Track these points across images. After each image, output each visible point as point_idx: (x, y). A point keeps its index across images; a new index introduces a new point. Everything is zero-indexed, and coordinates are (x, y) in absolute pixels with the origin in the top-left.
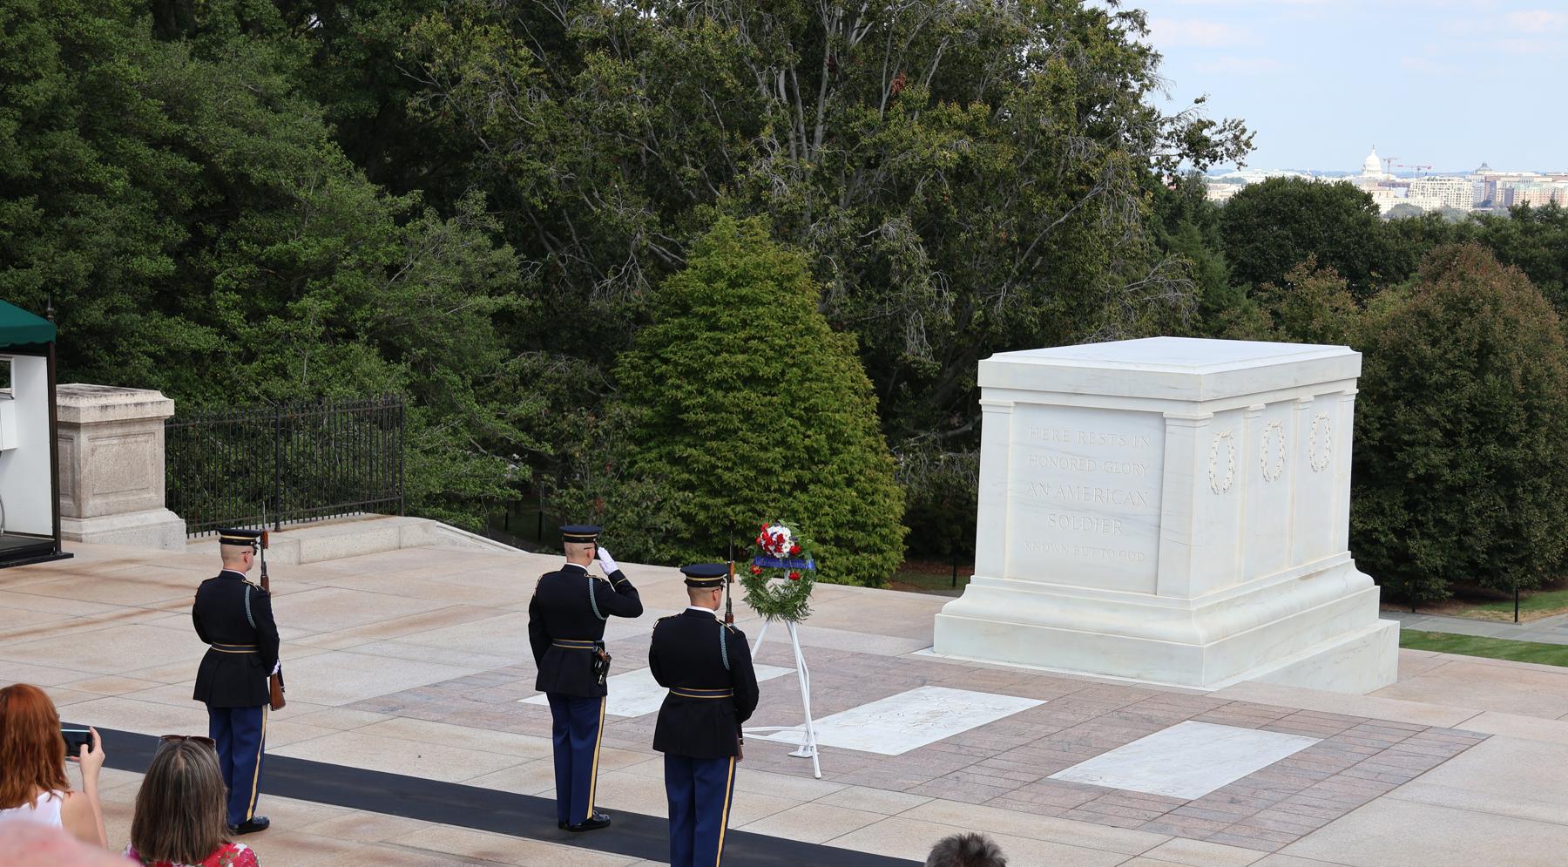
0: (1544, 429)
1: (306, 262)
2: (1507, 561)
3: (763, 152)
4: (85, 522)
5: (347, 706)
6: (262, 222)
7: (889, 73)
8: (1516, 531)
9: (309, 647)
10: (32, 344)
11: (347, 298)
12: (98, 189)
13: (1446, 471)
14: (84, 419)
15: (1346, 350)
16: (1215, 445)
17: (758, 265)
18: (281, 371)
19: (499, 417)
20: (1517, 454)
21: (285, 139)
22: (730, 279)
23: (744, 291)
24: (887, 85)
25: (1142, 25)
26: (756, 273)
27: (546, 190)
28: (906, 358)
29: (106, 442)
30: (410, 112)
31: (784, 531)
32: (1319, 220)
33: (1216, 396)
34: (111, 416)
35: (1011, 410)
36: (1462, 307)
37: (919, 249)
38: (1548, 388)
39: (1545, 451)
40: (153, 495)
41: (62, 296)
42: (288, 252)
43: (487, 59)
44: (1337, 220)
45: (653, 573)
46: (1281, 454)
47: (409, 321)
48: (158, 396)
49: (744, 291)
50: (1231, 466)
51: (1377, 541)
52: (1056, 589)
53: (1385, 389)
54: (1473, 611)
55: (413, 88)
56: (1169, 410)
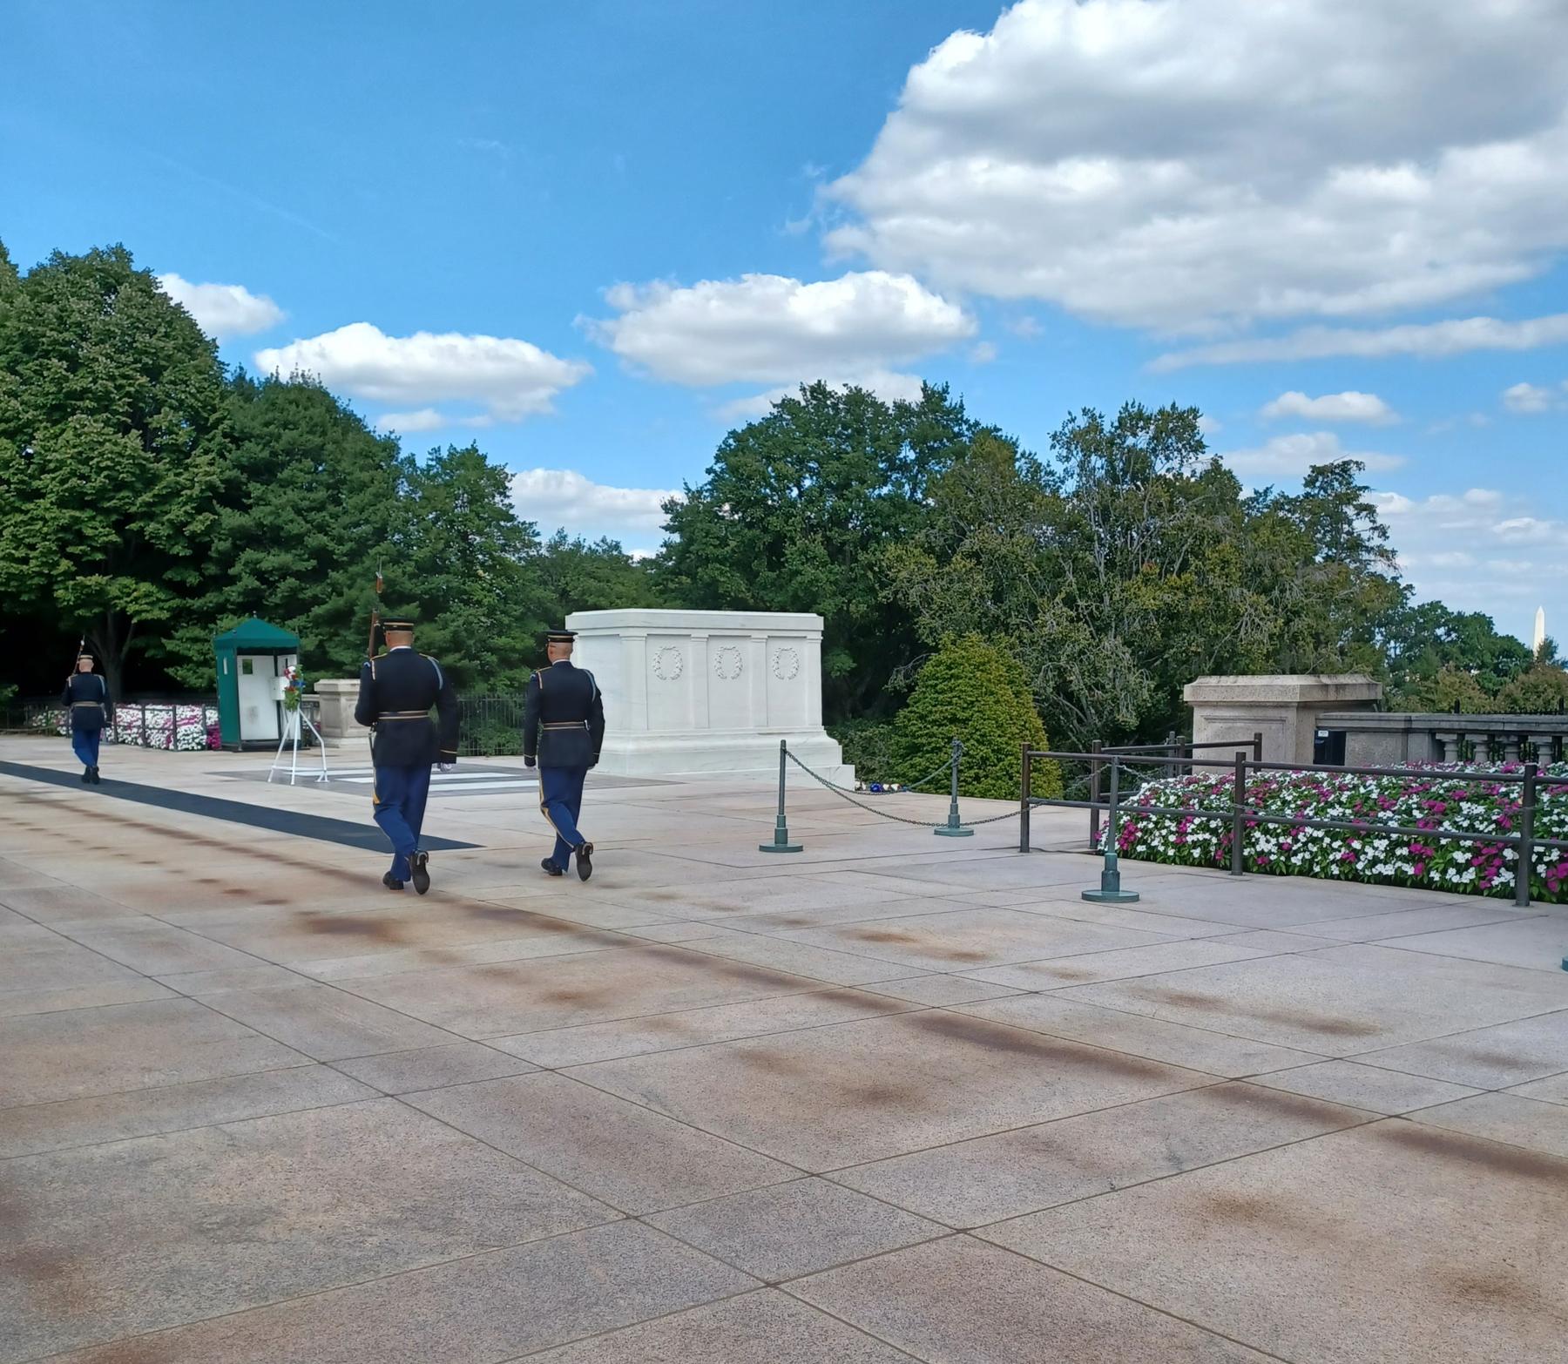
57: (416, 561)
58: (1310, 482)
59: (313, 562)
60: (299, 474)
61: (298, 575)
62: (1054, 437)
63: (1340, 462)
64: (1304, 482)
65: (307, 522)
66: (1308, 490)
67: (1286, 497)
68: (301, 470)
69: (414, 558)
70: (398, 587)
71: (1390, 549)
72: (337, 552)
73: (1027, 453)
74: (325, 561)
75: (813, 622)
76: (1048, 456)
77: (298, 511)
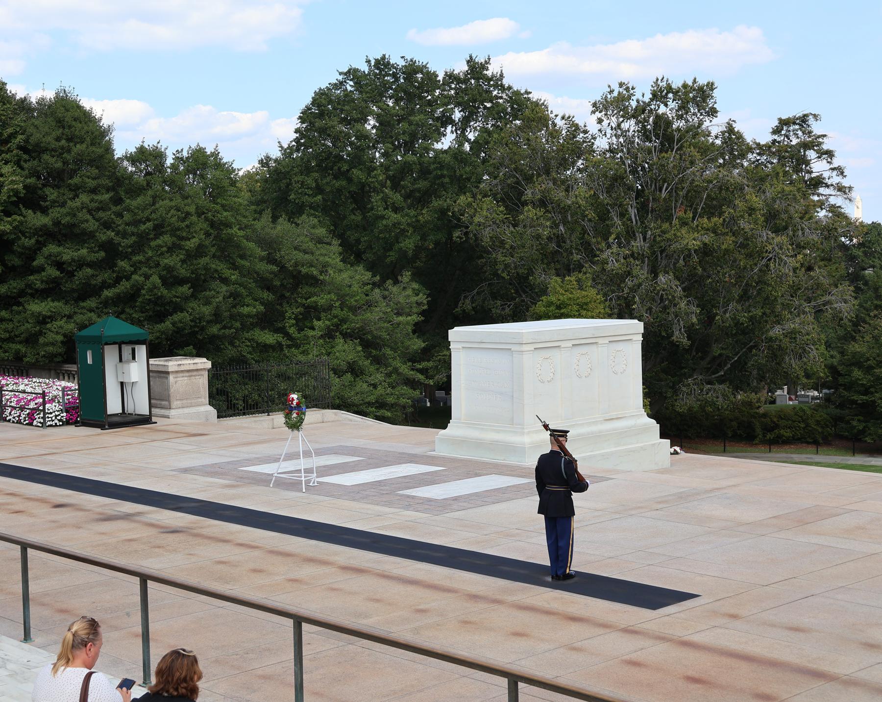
1: (321, 305)
3: (609, 246)
4: (172, 411)
6: (306, 289)
9: (194, 452)
10: (138, 340)
12: (225, 281)
14: (170, 370)
16: (539, 362)
17: (570, 298)
18: (305, 353)
19: (413, 370)
21: (321, 255)
22: (557, 305)
23: (562, 311)
24: (675, 211)
28: (673, 340)
29: (182, 379)
31: (294, 396)
33: (534, 341)
34: (182, 368)
35: (461, 350)
37: (678, 288)
40: (203, 400)
41: (200, 323)
42: (315, 302)
45: (416, 430)
46: (590, 365)
47: (370, 329)
48: (204, 360)
49: (562, 311)
50: (553, 370)
52: (479, 424)
55: (457, 226)
56: (514, 348)
57: (187, 251)
59: (102, 254)
60: (87, 180)
61: (91, 265)
62: (594, 105)
65: (97, 220)
69: (187, 248)
70: (175, 273)
72: (123, 244)
74: (112, 251)
75: (634, 328)
77: (90, 212)
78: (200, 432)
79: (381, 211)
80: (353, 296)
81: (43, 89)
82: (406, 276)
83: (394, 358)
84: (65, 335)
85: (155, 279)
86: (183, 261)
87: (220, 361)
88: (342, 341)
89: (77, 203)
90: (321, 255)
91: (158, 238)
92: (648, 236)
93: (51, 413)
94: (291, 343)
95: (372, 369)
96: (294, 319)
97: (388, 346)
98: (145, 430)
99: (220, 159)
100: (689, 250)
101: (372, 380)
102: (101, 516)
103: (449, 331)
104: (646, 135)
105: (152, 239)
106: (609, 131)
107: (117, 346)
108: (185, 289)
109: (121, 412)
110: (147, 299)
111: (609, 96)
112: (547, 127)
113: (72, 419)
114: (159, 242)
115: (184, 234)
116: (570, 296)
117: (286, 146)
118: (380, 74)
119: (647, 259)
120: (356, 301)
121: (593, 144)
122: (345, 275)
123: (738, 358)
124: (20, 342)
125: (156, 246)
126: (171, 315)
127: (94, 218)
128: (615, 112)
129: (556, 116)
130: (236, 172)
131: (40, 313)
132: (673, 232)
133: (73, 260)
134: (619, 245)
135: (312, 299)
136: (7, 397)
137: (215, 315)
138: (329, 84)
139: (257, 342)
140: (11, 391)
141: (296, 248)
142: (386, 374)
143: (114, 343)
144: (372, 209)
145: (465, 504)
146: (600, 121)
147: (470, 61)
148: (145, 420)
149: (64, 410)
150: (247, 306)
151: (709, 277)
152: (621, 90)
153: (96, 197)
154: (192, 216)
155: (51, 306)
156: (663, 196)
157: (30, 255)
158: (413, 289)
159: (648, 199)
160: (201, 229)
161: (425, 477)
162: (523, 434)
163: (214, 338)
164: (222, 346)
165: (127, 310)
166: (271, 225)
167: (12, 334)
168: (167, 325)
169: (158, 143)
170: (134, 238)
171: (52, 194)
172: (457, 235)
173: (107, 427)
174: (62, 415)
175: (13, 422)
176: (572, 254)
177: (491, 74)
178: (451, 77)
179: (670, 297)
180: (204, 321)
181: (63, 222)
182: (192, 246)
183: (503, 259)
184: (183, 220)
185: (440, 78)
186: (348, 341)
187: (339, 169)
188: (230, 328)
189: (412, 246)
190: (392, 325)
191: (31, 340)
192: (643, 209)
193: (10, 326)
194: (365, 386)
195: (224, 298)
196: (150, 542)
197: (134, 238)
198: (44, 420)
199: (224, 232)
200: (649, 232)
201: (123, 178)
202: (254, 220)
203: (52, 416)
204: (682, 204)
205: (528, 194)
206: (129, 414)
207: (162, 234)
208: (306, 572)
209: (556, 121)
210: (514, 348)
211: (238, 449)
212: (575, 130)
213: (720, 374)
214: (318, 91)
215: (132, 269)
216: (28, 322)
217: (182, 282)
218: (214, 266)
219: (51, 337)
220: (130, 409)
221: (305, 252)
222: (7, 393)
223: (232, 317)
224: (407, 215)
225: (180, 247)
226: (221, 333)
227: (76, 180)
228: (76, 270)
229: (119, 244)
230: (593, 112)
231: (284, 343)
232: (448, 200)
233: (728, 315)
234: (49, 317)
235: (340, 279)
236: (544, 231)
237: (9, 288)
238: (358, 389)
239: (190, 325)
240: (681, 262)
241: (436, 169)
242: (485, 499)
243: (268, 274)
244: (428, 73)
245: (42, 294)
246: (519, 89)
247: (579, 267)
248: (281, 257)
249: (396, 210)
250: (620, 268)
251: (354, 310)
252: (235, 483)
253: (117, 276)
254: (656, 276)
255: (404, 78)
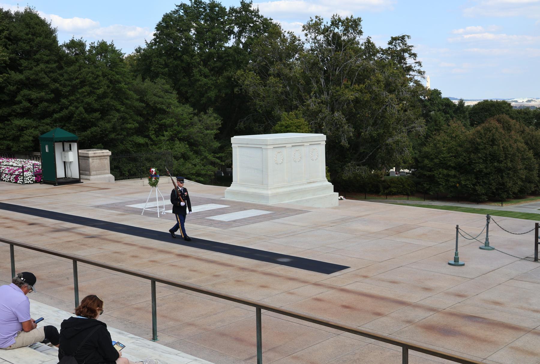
0: (509, 159)
2: (502, 191)
3: (311, 98)
4: (91, 176)
5: (91, 206)
6: (160, 116)
7: (343, 79)
8: (503, 184)
11: (177, 132)
12: (118, 111)
13: (485, 170)
15: (322, 135)
17: (292, 123)
18: (160, 148)
19: (214, 157)
20: (502, 165)
21: (168, 98)
23: (288, 129)
25: (420, 65)
26: (291, 125)
27: (262, 108)
29: (95, 160)
30: (235, 92)
31: (153, 170)
32: (496, 110)
33: (273, 144)
34: (96, 155)
36: (488, 130)
38: (510, 149)
39: (509, 164)
40: (107, 171)
41: (105, 132)
42: (164, 122)
43: (250, 79)
44: (501, 110)
46: (300, 156)
48: (108, 151)
49: (288, 129)
50: (282, 158)
51: (468, 187)
53: (469, 150)
54: (493, 204)
55: (236, 86)
56: (263, 147)
57: (98, 95)
58: (390, 43)
59: (53, 95)
60: (44, 56)
61: (47, 101)
62: (304, 27)
63: (401, 35)
64: (388, 43)
65: (50, 78)
66: (390, 46)
67: (382, 49)
68: (44, 55)
69: (98, 93)
70: (92, 106)
71: (422, 71)
72: (64, 91)
73: (290, 32)
74: (58, 95)
76: (300, 33)
77: (45, 73)
78: (106, 187)
79: (198, 77)
80: (184, 120)
81: (18, 7)
82: (210, 110)
83: (205, 152)
84: (34, 137)
85: (81, 109)
86: (96, 100)
87: (116, 152)
88: (178, 142)
89: (39, 68)
90: (168, 98)
91: (82, 88)
92: (330, 93)
93: (27, 177)
94: (152, 143)
95: (194, 156)
96: (154, 131)
97: (202, 145)
98: (77, 186)
99: (115, 48)
100: (349, 100)
101: (193, 162)
102: (53, 230)
103: (231, 138)
104: (328, 43)
105: (79, 88)
106: (311, 40)
107: (62, 143)
108: (97, 115)
109: (64, 176)
110: (77, 119)
111: (311, 23)
112: (281, 37)
113: (38, 180)
114: (83, 90)
115: (96, 86)
116: (292, 122)
117: (149, 42)
118: (197, 7)
119: (329, 104)
120: (185, 122)
121: (303, 46)
122: (179, 109)
123: (372, 153)
124: (10, 140)
125: (82, 92)
126: (90, 128)
127: (48, 76)
128: (314, 31)
129: (285, 32)
130: (123, 55)
131: (20, 126)
132: (341, 91)
133: (37, 98)
134: (316, 97)
135: (163, 121)
136: (3, 168)
137: (113, 128)
138: (171, 11)
139: (135, 142)
140: (5, 165)
141: (154, 95)
142: (201, 159)
143: (60, 141)
144: (193, 76)
145: (239, 224)
146: (306, 35)
147: (242, 3)
148: (77, 181)
149: (34, 176)
150: (130, 124)
151: (358, 114)
152: (317, 20)
153: (48, 66)
154: (100, 77)
155: (26, 122)
156: (337, 73)
157: (14, 94)
158: (214, 117)
159: (330, 75)
160: (105, 84)
161: (220, 210)
162: (268, 189)
163: (113, 139)
164: (117, 144)
165: (67, 125)
166: (142, 83)
167: (5, 136)
168: (88, 132)
169: (82, 38)
170: (69, 88)
171: (25, 63)
172: (236, 90)
173: (57, 184)
174: (33, 178)
175: (7, 181)
176: (293, 101)
177: (253, 9)
178: (232, 10)
179: (340, 123)
180: (107, 131)
181: (31, 78)
182: (101, 92)
183: (259, 103)
184: (96, 79)
185: (227, 10)
186: (181, 142)
187: (177, 55)
188: (121, 135)
189: (214, 95)
190: (204, 134)
191: (15, 139)
192: (327, 80)
193: (4, 132)
194: (190, 165)
195: (117, 120)
196: (80, 243)
197: (69, 88)
198: (23, 180)
199: (117, 86)
200: (330, 91)
201: (63, 56)
202: (133, 80)
203: (27, 178)
204: (346, 78)
205: (271, 70)
206: (68, 178)
207: (85, 86)
208: (160, 257)
209: (285, 34)
210: (263, 147)
211: (125, 196)
212: (294, 39)
213: (363, 161)
214: (165, 14)
215: (69, 103)
216: (13, 130)
217: (95, 111)
218: (112, 103)
219: (26, 138)
220: (69, 175)
221: (159, 97)
222: (3, 166)
223: (122, 129)
224: (211, 79)
225: (94, 93)
226: (116, 138)
227: (38, 56)
228: (39, 103)
229: (62, 90)
230: (303, 30)
231: (149, 143)
232: (232, 72)
233: (367, 132)
234: (25, 127)
235: (177, 111)
236: (279, 89)
237: (2, 112)
238: (187, 167)
239: (100, 134)
240: (345, 106)
241: (226, 56)
242: (249, 221)
243: (140, 108)
244: (221, 7)
245: (21, 115)
246: (267, 17)
247: (296, 107)
248: (147, 99)
249: (206, 77)
250: (316, 109)
251: (184, 127)
252: (124, 213)
253: (61, 107)
254: (333, 113)
255: (209, 10)
